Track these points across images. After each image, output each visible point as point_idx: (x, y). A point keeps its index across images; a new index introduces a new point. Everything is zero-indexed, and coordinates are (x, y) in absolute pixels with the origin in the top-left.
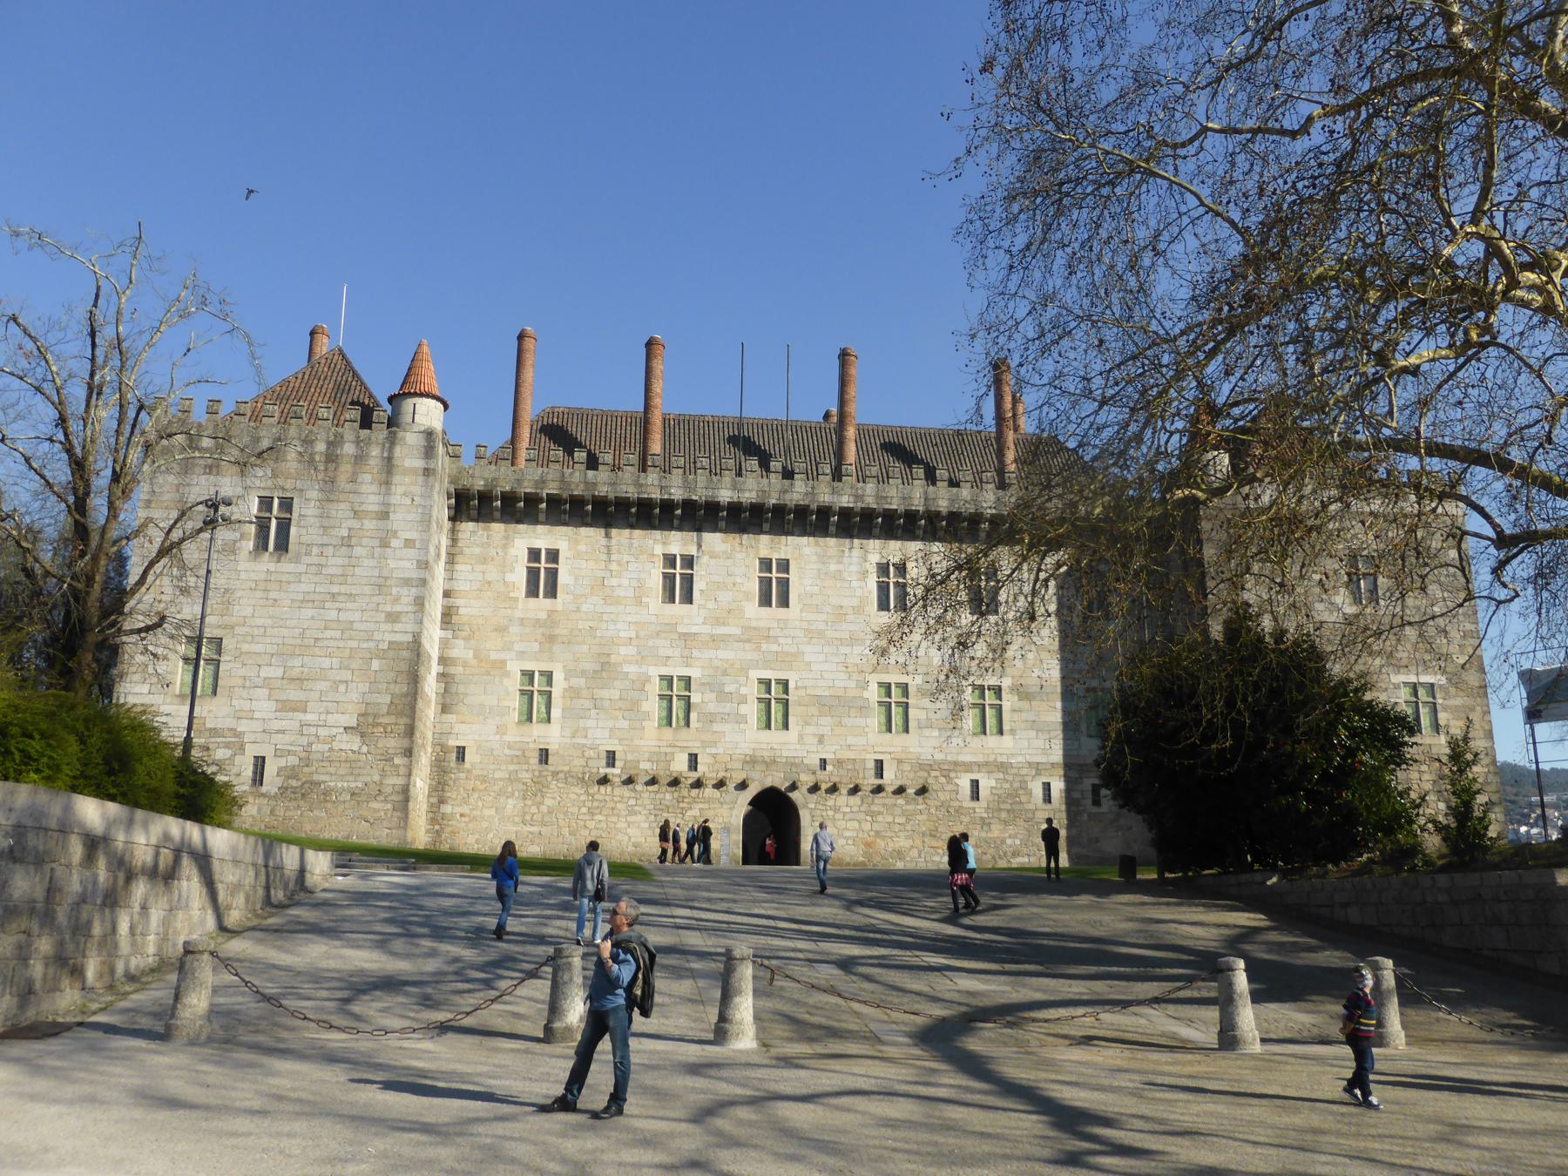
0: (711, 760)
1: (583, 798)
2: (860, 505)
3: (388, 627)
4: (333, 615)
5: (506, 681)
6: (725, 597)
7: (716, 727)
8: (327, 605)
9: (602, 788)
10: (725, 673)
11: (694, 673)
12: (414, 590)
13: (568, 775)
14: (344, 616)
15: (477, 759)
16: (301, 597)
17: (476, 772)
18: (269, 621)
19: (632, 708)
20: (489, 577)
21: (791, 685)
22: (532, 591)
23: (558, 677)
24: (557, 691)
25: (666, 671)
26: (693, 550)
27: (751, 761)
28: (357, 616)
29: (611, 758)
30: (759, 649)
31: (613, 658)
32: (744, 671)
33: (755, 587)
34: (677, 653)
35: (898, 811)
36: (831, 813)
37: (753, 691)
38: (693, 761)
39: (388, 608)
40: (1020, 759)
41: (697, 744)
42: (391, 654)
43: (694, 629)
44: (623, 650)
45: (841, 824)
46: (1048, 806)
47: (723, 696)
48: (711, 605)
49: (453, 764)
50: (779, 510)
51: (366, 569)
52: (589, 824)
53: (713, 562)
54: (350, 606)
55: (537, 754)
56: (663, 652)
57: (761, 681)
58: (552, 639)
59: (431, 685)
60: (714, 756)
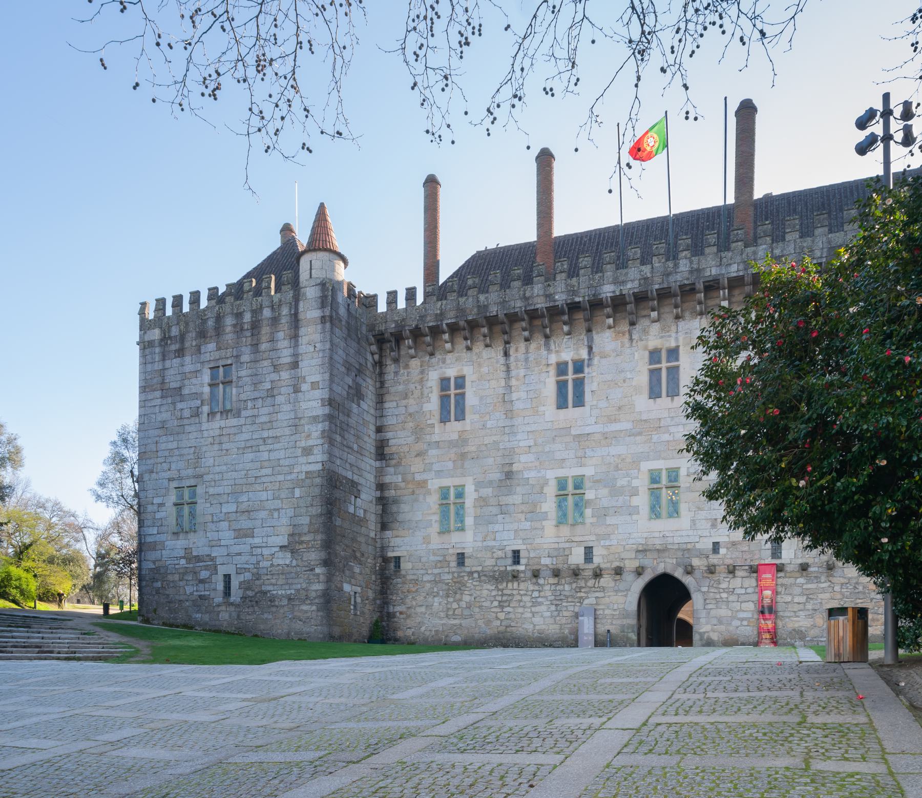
0: (605, 552)
1: (494, 593)
3: (303, 460)
4: (265, 456)
7: (609, 520)
8: (262, 448)
9: (510, 585)
11: (588, 471)
12: (320, 425)
14: (274, 456)
16: (243, 445)
17: (409, 577)
18: (224, 468)
20: (411, 410)
23: (470, 489)
25: (561, 473)
27: (643, 551)
28: (282, 454)
31: (515, 468)
36: (724, 595)
38: (589, 551)
39: (303, 444)
41: (593, 538)
42: (308, 481)
44: (523, 458)
47: (615, 491)
51: (285, 416)
54: (277, 446)
55: (454, 558)
56: (558, 455)
58: (463, 456)
59: (364, 503)
60: (607, 547)
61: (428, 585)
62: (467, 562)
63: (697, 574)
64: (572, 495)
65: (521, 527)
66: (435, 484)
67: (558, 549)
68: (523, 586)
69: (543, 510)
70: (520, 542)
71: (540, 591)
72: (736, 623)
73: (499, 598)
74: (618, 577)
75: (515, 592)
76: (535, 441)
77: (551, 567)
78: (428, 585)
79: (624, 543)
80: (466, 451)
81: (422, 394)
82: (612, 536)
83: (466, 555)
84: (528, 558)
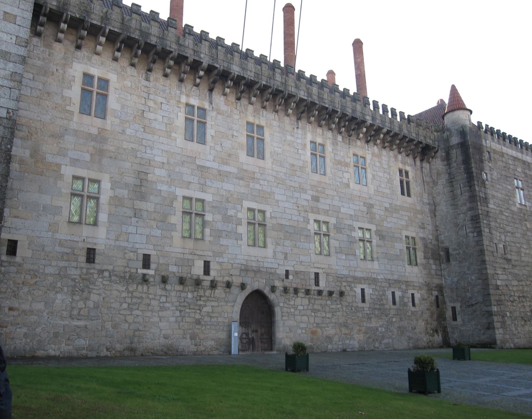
0: (218, 267)
1: (124, 295)
2: (310, 99)
5: (60, 184)
6: (227, 144)
7: (223, 241)
9: (140, 287)
10: (228, 201)
11: (208, 197)
12: (11, 65)
13: (112, 273)
15: (29, 254)
19: (163, 219)
21: (268, 215)
22: (85, 110)
24: (104, 199)
26: (206, 105)
27: (245, 270)
29: (146, 261)
30: (248, 186)
32: (240, 201)
33: (243, 140)
34: (196, 180)
35: (327, 309)
36: (292, 310)
37: (243, 215)
40: (382, 277)
41: (210, 254)
43: (208, 164)
44: (157, 171)
45: (298, 318)
46: (394, 307)
48: (218, 148)
49: (4, 258)
50: (264, 89)
52: (130, 319)
53: (220, 117)
55: (84, 253)
56: (186, 178)
57: (249, 209)
58: (101, 153)
60: (220, 264)
61: (51, 278)
62: (98, 259)
63: (278, 292)
64: (194, 212)
65: (153, 233)
66: (68, 171)
67: (183, 259)
68: (152, 290)
69: (172, 222)
70: (151, 247)
71: (167, 297)
72: (299, 331)
73: (129, 300)
74: (228, 290)
75: (144, 295)
76: (168, 160)
77: (177, 275)
78: (51, 278)
79: (232, 262)
80: (105, 148)
81: (63, 78)
82: (224, 255)
83: (97, 251)
84: (158, 264)
